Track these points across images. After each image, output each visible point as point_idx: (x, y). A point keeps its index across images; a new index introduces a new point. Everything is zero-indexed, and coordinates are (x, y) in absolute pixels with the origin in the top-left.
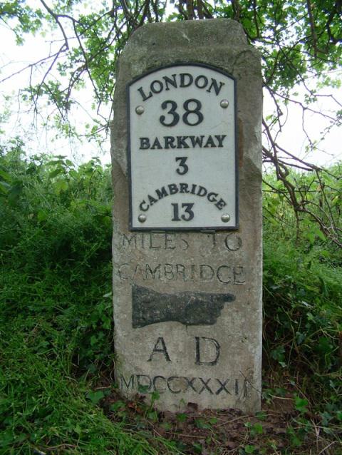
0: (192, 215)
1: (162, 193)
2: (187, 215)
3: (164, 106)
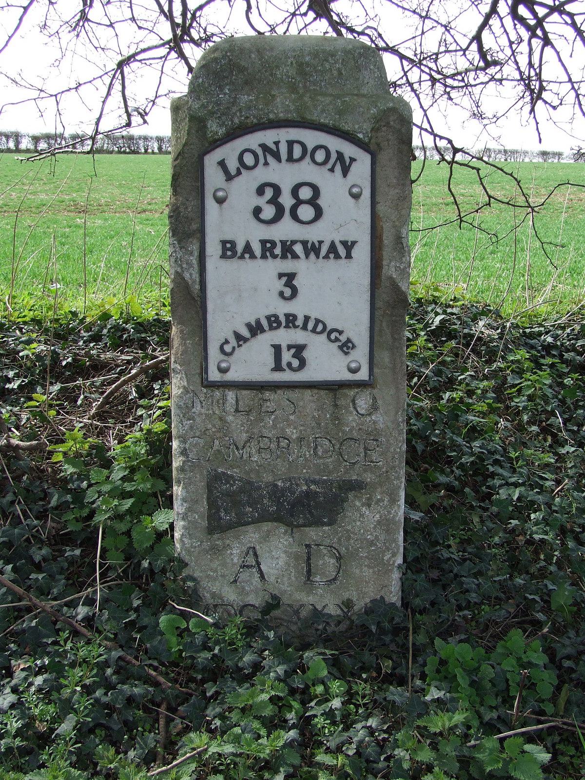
0: (303, 363)
1: (256, 329)
2: (296, 363)
3: (260, 191)
